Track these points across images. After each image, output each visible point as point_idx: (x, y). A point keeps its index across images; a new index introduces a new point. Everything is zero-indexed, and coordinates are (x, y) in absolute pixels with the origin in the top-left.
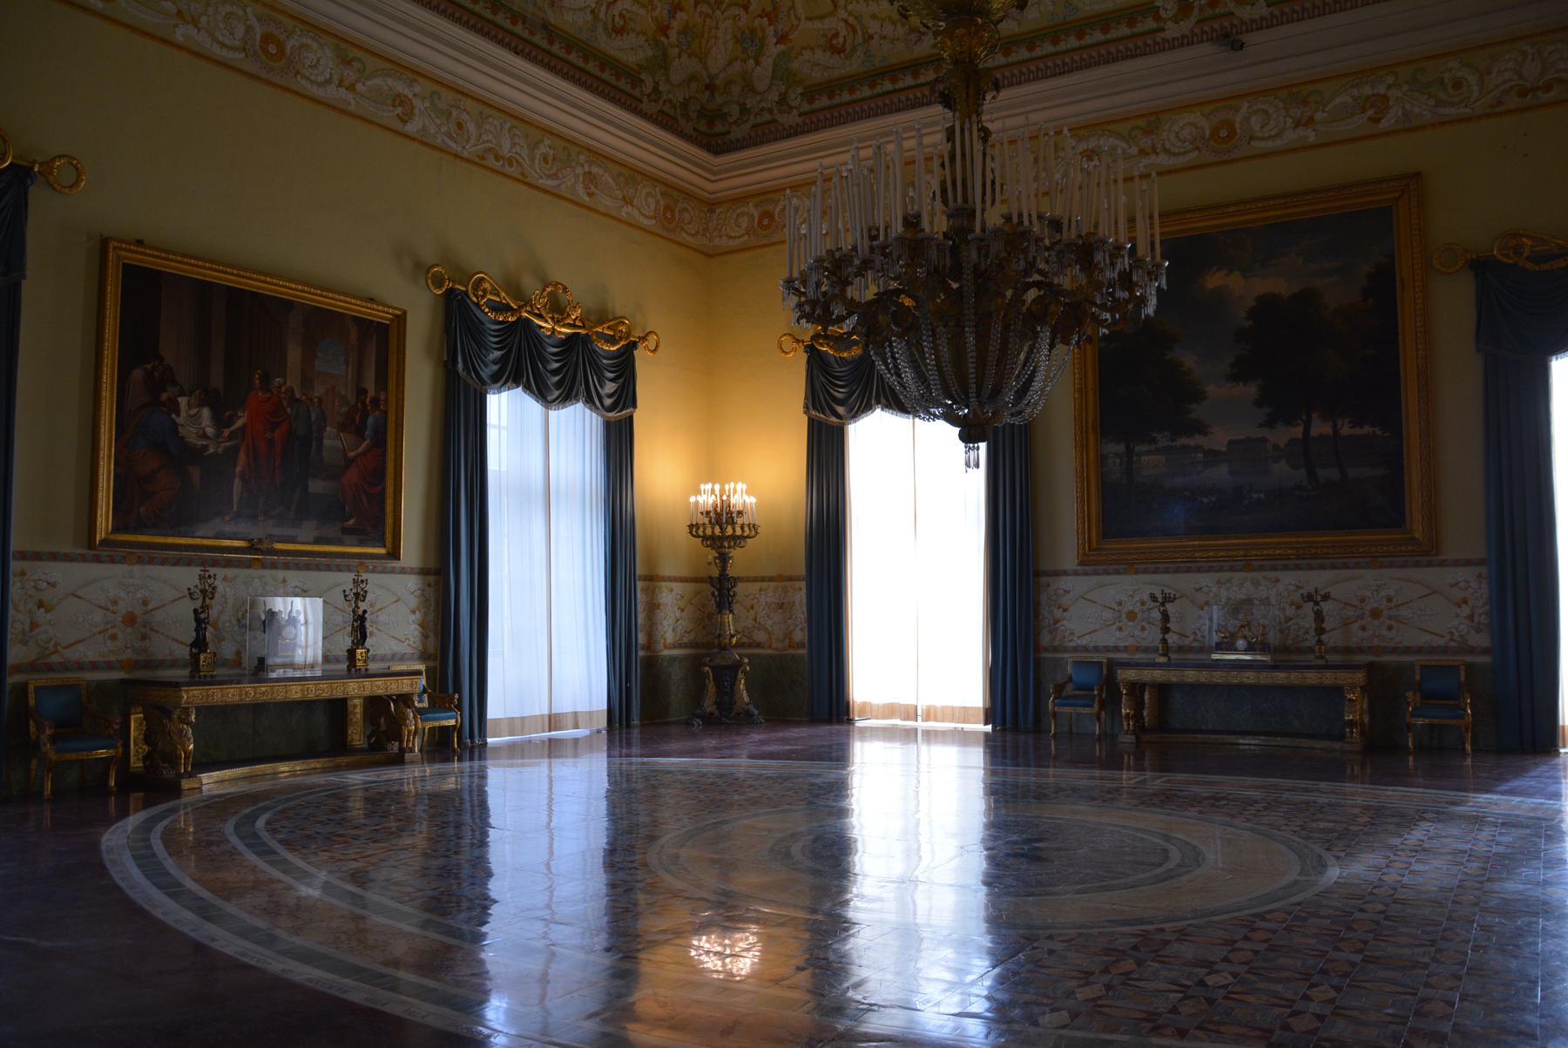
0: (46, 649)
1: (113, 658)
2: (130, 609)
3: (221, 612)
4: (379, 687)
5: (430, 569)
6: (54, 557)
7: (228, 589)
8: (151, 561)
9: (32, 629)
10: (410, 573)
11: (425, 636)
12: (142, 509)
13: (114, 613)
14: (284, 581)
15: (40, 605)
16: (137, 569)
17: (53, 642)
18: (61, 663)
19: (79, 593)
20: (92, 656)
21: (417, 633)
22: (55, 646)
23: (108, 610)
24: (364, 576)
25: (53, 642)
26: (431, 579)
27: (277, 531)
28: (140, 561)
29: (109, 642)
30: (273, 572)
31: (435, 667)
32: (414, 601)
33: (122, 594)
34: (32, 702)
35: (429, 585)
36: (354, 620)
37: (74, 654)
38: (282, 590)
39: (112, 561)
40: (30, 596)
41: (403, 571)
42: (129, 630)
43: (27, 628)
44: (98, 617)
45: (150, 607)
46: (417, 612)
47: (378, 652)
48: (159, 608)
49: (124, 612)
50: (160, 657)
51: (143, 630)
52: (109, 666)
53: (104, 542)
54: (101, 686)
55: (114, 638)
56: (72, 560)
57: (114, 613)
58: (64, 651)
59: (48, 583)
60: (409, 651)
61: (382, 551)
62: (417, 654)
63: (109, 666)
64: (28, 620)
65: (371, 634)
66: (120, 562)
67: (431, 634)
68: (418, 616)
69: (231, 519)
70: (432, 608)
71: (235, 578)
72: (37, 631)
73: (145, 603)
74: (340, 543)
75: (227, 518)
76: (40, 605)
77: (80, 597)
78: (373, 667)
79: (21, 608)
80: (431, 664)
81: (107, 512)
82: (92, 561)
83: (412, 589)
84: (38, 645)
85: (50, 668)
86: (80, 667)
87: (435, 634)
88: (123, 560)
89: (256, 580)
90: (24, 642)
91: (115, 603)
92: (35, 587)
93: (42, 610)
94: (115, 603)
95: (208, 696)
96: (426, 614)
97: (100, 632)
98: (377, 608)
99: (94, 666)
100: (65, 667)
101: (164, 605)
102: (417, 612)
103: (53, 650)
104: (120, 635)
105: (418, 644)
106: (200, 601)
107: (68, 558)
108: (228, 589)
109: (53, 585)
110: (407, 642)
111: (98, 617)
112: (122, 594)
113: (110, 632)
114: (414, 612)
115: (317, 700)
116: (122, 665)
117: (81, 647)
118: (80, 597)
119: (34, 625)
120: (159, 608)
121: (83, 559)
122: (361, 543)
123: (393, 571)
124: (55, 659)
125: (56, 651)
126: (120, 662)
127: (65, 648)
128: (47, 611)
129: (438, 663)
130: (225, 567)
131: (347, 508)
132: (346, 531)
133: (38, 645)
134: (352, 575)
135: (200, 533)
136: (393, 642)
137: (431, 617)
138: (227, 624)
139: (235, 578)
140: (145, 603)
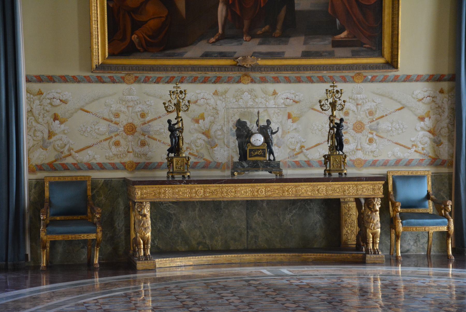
0: (294, 150)
1: (116, 161)
2: (130, 121)
3: (212, 123)
4: (334, 190)
5: (443, 76)
6: (64, 79)
7: (219, 102)
8: (147, 81)
9: (50, 137)
10: (417, 81)
11: (438, 143)
12: (134, 37)
13: (117, 124)
14: (275, 93)
15: (56, 118)
16: (135, 87)
17: (67, 148)
18: (74, 164)
19: (86, 108)
20: (100, 159)
21: (427, 140)
22: (69, 150)
23: (112, 122)
24: (340, 86)
25: (67, 148)
26: (445, 85)
27: (264, 49)
28: (137, 80)
29: (113, 147)
30: (263, 86)
31: (450, 175)
32: (422, 109)
33: (124, 109)
34: (47, 194)
35: (442, 92)
36: (331, 129)
37: (84, 157)
38: (272, 102)
39: (113, 81)
40: (47, 111)
41: (408, 79)
42: (130, 137)
43: (46, 136)
44: (103, 127)
45: (148, 119)
46: (427, 119)
47: (380, 158)
48: (155, 119)
49: (125, 123)
50: (159, 160)
51: (142, 138)
52: (114, 167)
53: (102, 67)
54: (107, 182)
55: (117, 144)
56: (79, 82)
57: (117, 124)
58: (77, 155)
59: (61, 101)
60: (417, 157)
61: (380, 60)
62: (427, 160)
63: (114, 167)
64: (47, 131)
65: (348, 142)
66: (119, 82)
67: (445, 142)
68: (428, 123)
69: (217, 40)
70: (446, 114)
71: (226, 92)
72: (53, 138)
73: (143, 115)
74: (331, 55)
75: (213, 40)
76: (56, 118)
77: (87, 112)
78: (350, 172)
79: (40, 120)
80: (444, 170)
81: (103, 41)
82: (96, 82)
83: (420, 97)
84: (55, 149)
85: (65, 168)
86: (90, 167)
87: (450, 140)
88: (123, 80)
89: (246, 93)
90: (44, 147)
91: (117, 115)
92: (51, 104)
93: (57, 122)
94: (117, 115)
95: (160, 193)
96: (437, 121)
97: (106, 140)
98: (377, 116)
99: (102, 167)
100: (77, 167)
101: (160, 117)
102: (427, 119)
103: (67, 153)
104: (122, 142)
105: (428, 150)
106: (174, 115)
107: (75, 80)
108: (219, 102)
109: (64, 102)
110: (414, 148)
111: (103, 127)
112: (124, 109)
113: (114, 140)
114: (422, 119)
115: (311, 200)
116: (124, 167)
117: (90, 151)
118: (87, 112)
119: (51, 134)
120: (155, 119)
121: (88, 80)
122: (355, 55)
123: (396, 79)
124: (69, 160)
125: (70, 155)
126: (123, 164)
127: (77, 152)
128: (61, 123)
129: (453, 170)
130: (215, 82)
131: (338, 21)
132: (336, 44)
133: (55, 149)
134: (327, 86)
135: (188, 55)
136: (397, 149)
137: (445, 122)
138: (219, 133)
139: (226, 92)
140: (143, 115)
